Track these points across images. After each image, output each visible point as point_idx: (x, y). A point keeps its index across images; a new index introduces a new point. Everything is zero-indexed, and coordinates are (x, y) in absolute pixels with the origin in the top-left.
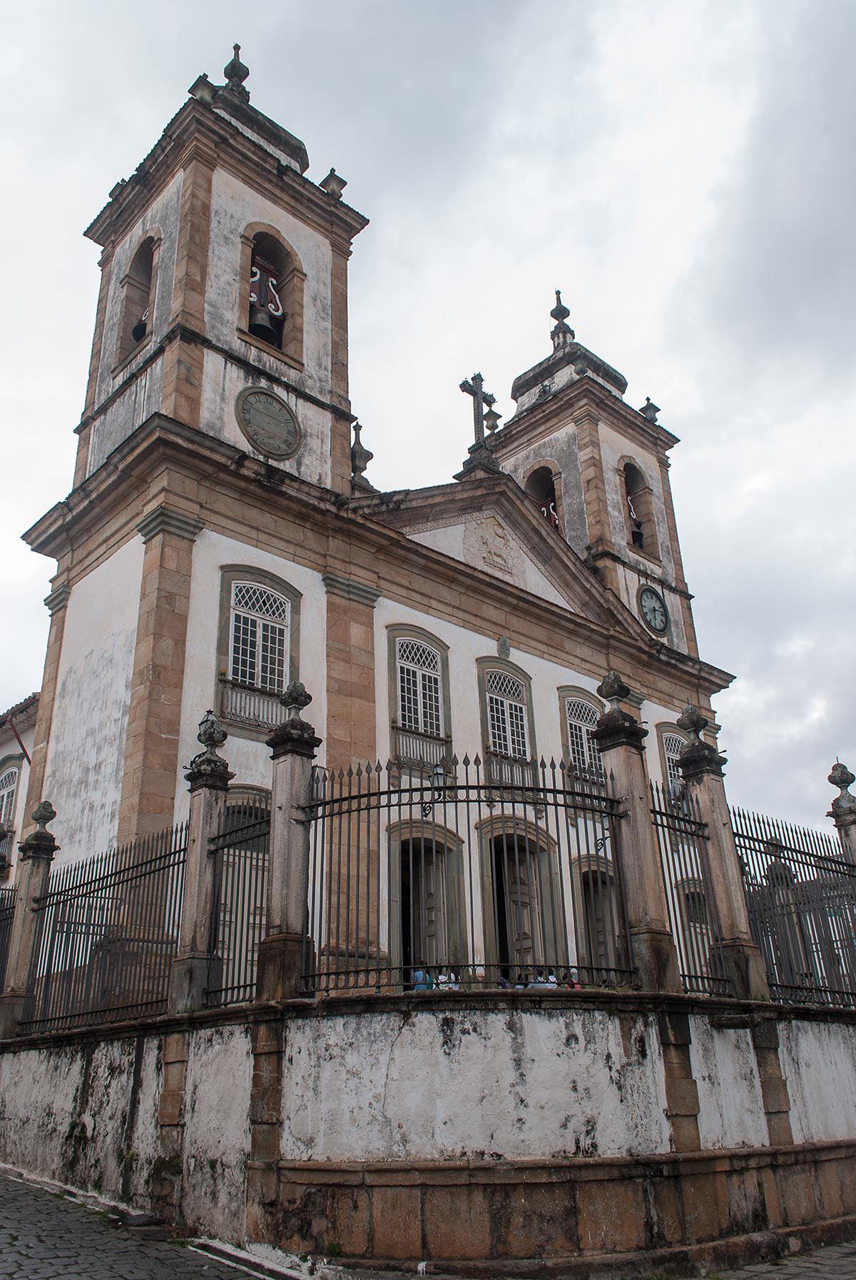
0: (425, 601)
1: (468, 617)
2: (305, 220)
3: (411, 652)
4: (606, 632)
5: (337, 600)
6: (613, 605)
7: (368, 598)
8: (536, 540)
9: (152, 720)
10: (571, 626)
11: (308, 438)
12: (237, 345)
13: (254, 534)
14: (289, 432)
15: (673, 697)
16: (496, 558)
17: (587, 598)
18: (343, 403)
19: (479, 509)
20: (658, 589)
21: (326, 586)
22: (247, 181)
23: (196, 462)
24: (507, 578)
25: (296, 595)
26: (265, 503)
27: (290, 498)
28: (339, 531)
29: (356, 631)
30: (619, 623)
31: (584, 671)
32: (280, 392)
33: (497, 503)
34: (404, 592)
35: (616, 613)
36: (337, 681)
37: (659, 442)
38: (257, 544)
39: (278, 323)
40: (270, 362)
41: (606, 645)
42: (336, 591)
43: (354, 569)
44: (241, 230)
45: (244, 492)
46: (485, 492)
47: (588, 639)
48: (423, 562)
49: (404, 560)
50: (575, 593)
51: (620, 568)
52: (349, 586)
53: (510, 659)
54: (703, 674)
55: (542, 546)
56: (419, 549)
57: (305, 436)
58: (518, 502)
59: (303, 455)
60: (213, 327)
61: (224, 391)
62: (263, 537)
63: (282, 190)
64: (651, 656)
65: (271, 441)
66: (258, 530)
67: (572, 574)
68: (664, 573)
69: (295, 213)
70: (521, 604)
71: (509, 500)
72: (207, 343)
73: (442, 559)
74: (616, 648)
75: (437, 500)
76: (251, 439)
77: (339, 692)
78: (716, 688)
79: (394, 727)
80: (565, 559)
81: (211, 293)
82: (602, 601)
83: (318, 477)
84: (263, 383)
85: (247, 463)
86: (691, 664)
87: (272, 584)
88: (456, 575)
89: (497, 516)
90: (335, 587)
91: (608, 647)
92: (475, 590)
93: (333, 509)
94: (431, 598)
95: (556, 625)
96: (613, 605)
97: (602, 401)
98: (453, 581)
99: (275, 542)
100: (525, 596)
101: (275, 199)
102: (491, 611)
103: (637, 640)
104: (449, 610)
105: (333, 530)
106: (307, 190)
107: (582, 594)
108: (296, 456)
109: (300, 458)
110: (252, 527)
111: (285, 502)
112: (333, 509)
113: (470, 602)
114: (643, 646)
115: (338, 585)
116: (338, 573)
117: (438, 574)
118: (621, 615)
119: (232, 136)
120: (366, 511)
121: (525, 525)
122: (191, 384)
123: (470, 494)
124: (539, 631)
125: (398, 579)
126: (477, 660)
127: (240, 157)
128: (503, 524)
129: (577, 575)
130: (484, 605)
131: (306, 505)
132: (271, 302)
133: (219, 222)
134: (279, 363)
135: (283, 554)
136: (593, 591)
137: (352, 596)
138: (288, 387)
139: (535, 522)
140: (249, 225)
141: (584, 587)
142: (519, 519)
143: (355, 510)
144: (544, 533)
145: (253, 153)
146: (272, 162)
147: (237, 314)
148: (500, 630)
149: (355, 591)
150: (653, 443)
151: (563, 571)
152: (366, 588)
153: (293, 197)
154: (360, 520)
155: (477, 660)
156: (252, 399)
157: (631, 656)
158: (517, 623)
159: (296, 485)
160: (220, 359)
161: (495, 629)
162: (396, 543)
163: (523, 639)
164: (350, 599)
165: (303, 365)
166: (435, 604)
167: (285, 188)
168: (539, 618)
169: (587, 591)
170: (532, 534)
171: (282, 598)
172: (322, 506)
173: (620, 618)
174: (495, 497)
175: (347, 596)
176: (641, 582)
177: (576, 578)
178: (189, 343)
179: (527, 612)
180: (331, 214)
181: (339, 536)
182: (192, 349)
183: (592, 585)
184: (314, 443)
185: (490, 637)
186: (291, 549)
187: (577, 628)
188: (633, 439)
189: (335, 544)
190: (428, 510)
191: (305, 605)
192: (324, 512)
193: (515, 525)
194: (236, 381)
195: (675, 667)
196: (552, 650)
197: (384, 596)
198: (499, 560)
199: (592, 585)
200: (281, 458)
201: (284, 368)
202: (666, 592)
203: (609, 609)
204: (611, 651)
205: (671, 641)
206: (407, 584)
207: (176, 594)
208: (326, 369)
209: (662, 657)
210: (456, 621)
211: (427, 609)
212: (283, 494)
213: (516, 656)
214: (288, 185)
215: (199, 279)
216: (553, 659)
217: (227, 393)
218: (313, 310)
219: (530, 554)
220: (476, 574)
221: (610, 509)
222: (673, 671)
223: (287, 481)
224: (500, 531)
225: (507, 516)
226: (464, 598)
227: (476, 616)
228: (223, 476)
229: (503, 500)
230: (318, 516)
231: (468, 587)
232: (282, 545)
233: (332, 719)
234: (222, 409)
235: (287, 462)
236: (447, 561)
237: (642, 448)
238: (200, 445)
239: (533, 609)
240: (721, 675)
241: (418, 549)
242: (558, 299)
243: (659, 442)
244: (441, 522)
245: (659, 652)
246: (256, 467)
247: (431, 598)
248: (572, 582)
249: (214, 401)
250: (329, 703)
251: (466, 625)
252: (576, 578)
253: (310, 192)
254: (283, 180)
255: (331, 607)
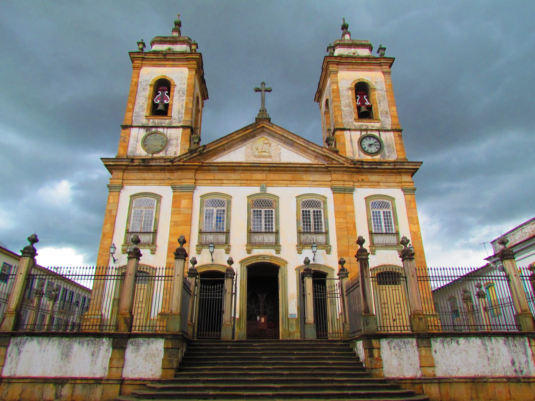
0: (220, 182)
1: (242, 182)
2: (177, 66)
3: (215, 203)
4: (324, 166)
5: (177, 193)
6: (328, 153)
7: (193, 189)
8: (284, 139)
9: (101, 250)
10: (304, 169)
11: (171, 141)
12: (144, 121)
13: (144, 182)
14: (163, 142)
15: (380, 182)
16: (263, 154)
17: (316, 154)
18: (187, 123)
19: (254, 136)
20: (376, 134)
21: (173, 189)
22: (154, 66)
23: (119, 167)
24: (269, 160)
25: (159, 198)
26: (148, 170)
27: (154, 166)
28: (177, 170)
29: (184, 203)
30: (333, 159)
31: (314, 186)
32: (161, 130)
33: (263, 131)
34: (210, 182)
35: (330, 156)
36: (174, 222)
37: (382, 64)
38: (145, 184)
39: (167, 106)
40: (157, 121)
41: (327, 170)
42: (176, 191)
43: (183, 181)
44: (150, 83)
45: (139, 170)
46: (251, 130)
47: (317, 171)
48: (217, 168)
49: (210, 170)
50: (309, 153)
51: (347, 134)
52: (181, 187)
53: (268, 192)
54: (397, 167)
55: (287, 140)
56: (212, 164)
57: (170, 140)
58: (270, 128)
59: (168, 148)
60: (136, 120)
61: (137, 139)
62: (147, 181)
63: (168, 61)
64: (357, 168)
65: (155, 148)
66: (145, 180)
67: (305, 147)
68: (382, 124)
69: (173, 66)
70: (271, 168)
71: (267, 128)
72: (132, 127)
73: (224, 164)
74: (334, 171)
75: (223, 143)
76: (147, 151)
77: (174, 225)
78: (415, 171)
79: (201, 232)
80: (299, 142)
81: (136, 109)
82: (322, 153)
83: (174, 153)
84: (154, 130)
85: (135, 161)
86: (387, 164)
87: (150, 196)
88: (234, 168)
89: (264, 136)
90: (175, 189)
91: (329, 171)
92: (247, 170)
93: (170, 164)
94: (223, 180)
95: (296, 171)
96: (328, 153)
97: (339, 62)
98: (235, 170)
99: (152, 181)
100: (271, 165)
101: (164, 66)
102: (258, 176)
103: (344, 164)
104: (233, 182)
105: (175, 170)
106: (175, 56)
107: (313, 153)
108: (165, 149)
109: (167, 149)
110: (143, 180)
111: (153, 168)
112: (170, 164)
113: (246, 175)
114: (349, 166)
115: (176, 188)
116: (177, 184)
117: (227, 170)
118: (333, 155)
119: (145, 55)
120: (185, 159)
121: (277, 135)
122: (125, 142)
123: (243, 134)
124: (287, 176)
125: (208, 178)
126: (247, 197)
127: (151, 60)
128: (268, 138)
129: (307, 146)
130: (254, 174)
131: (161, 166)
132: (165, 99)
133: (141, 85)
134: (161, 120)
135: (156, 184)
136: (317, 150)
137: (183, 191)
138: (163, 127)
139: (280, 133)
140: (153, 80)
141: (312, 150)
142: (274, 134)
143: (179, 161)
144: (286, 135)
145: (154, 56)
146: (161, 55)
147: (145, 111)
148: (261, 182)
149: (183, 188)
150: (379, 66)
151: (300, 146)
152: (188, 186)
153: (173, 61)
154: (181, 164)
155: (247, 197)
156: (148, 137)
157: (345, 171)
158: (272, 176)
159: (154, 161)
160: (137, 129)
161: (258, 182)
162: (202, 166)
163: (274, 182)
164: (182, 192)
165: (171, 117)
166: (225, 182)
167: (168, 60)
168: (284, 171)
169: (314, 151)
170: (281, 137)
171: (154, 199)
172: (166, 164)
173: (333, 157)
174: (260, 130)
175: (181, 191)
176: (362, 134)
177: (307, 148)
178: (125, 129)
179: (277, 171)
180: (187, 58)
181: (179, 171)
182: (127, 131)
183: (315, 148)
184: (174, 142)
185: (255, 186)
186: (159, 182)
187: (307, 169)
188: (357, 70)
189: (177, 175)
190: (222, 148)
191: (163, 200)
192: (168, 166)
193: (273, 137)
194: (142, 133)
195: (376, 168)
196: (294, 182)
197: (200, 186)
198: (266, 154)
199: (315, 148)
200: (158, 152)
201: (163, 121)
202: (382, 133)
203: (326, 155)
204: (332, 172)
205: (383, 156)
206: (212, 178)
207: (112, 210)
208: (182, 113)
209: (365, 167)
210: (236, 185)
211: (221, 184)
212: (151, 166)
213: (270, 190)
214: (169, 59)
215: (131, 107)
216: (294, 185)
217: (139, 139)
218: (178, 95)
219: (285, 146)
220: (242, 165)
221: (343, 108)
222: (377, 170)
223: (150, 161)
224: (266, 142)
225: (269, 135)
226: (242, 175)
227: (247, 180)
228: (129, 168)
229: (265, 129)
230: (167, 168)
231: (243, 170)
232: (155, 182)
233: (171, 235)
234: (136, 145)
235: (161, 153)
236: (226, 164)
237: (371, 71)
238: (117, 162)
239: (279, 169)
240: (411, 164)
241: (210, 165)
242: (344, 21)
243: (382, 64)
244: (232, 149)
245: (362, 165)
246: (138, 161)
247: (223, 180)
248: (307, 150)
249: (133, 144)
250: (170, 230)
251: (241, 185)
252: (307, 148)
253: (177, 56)
254: (166, 58)
255: (174, 197)
